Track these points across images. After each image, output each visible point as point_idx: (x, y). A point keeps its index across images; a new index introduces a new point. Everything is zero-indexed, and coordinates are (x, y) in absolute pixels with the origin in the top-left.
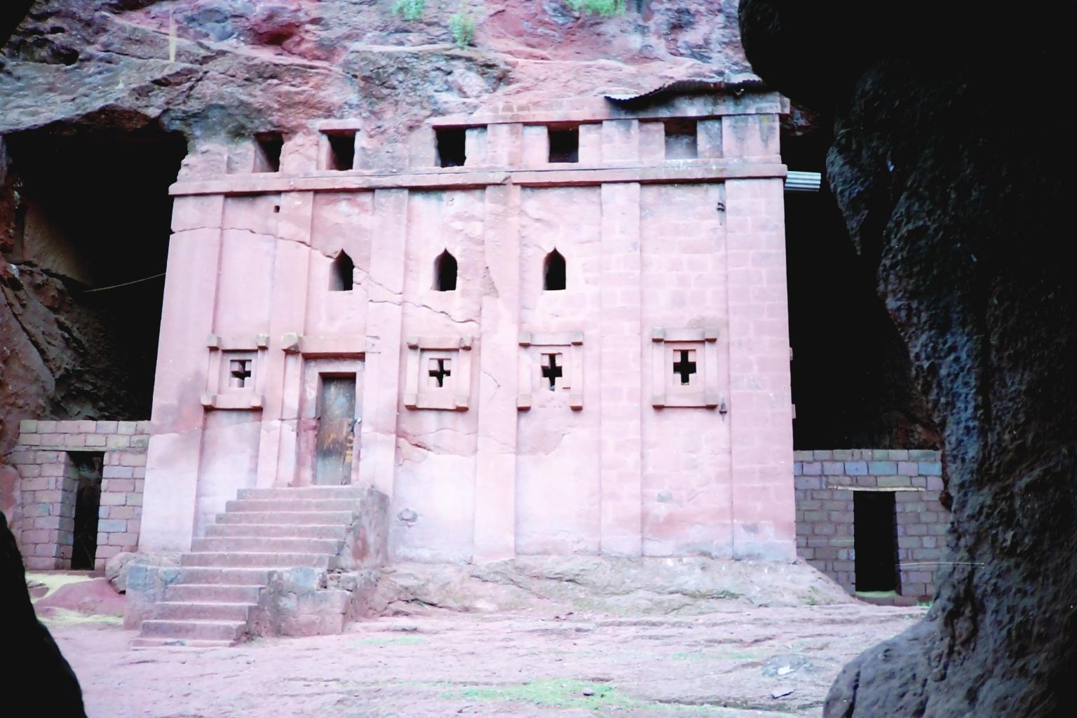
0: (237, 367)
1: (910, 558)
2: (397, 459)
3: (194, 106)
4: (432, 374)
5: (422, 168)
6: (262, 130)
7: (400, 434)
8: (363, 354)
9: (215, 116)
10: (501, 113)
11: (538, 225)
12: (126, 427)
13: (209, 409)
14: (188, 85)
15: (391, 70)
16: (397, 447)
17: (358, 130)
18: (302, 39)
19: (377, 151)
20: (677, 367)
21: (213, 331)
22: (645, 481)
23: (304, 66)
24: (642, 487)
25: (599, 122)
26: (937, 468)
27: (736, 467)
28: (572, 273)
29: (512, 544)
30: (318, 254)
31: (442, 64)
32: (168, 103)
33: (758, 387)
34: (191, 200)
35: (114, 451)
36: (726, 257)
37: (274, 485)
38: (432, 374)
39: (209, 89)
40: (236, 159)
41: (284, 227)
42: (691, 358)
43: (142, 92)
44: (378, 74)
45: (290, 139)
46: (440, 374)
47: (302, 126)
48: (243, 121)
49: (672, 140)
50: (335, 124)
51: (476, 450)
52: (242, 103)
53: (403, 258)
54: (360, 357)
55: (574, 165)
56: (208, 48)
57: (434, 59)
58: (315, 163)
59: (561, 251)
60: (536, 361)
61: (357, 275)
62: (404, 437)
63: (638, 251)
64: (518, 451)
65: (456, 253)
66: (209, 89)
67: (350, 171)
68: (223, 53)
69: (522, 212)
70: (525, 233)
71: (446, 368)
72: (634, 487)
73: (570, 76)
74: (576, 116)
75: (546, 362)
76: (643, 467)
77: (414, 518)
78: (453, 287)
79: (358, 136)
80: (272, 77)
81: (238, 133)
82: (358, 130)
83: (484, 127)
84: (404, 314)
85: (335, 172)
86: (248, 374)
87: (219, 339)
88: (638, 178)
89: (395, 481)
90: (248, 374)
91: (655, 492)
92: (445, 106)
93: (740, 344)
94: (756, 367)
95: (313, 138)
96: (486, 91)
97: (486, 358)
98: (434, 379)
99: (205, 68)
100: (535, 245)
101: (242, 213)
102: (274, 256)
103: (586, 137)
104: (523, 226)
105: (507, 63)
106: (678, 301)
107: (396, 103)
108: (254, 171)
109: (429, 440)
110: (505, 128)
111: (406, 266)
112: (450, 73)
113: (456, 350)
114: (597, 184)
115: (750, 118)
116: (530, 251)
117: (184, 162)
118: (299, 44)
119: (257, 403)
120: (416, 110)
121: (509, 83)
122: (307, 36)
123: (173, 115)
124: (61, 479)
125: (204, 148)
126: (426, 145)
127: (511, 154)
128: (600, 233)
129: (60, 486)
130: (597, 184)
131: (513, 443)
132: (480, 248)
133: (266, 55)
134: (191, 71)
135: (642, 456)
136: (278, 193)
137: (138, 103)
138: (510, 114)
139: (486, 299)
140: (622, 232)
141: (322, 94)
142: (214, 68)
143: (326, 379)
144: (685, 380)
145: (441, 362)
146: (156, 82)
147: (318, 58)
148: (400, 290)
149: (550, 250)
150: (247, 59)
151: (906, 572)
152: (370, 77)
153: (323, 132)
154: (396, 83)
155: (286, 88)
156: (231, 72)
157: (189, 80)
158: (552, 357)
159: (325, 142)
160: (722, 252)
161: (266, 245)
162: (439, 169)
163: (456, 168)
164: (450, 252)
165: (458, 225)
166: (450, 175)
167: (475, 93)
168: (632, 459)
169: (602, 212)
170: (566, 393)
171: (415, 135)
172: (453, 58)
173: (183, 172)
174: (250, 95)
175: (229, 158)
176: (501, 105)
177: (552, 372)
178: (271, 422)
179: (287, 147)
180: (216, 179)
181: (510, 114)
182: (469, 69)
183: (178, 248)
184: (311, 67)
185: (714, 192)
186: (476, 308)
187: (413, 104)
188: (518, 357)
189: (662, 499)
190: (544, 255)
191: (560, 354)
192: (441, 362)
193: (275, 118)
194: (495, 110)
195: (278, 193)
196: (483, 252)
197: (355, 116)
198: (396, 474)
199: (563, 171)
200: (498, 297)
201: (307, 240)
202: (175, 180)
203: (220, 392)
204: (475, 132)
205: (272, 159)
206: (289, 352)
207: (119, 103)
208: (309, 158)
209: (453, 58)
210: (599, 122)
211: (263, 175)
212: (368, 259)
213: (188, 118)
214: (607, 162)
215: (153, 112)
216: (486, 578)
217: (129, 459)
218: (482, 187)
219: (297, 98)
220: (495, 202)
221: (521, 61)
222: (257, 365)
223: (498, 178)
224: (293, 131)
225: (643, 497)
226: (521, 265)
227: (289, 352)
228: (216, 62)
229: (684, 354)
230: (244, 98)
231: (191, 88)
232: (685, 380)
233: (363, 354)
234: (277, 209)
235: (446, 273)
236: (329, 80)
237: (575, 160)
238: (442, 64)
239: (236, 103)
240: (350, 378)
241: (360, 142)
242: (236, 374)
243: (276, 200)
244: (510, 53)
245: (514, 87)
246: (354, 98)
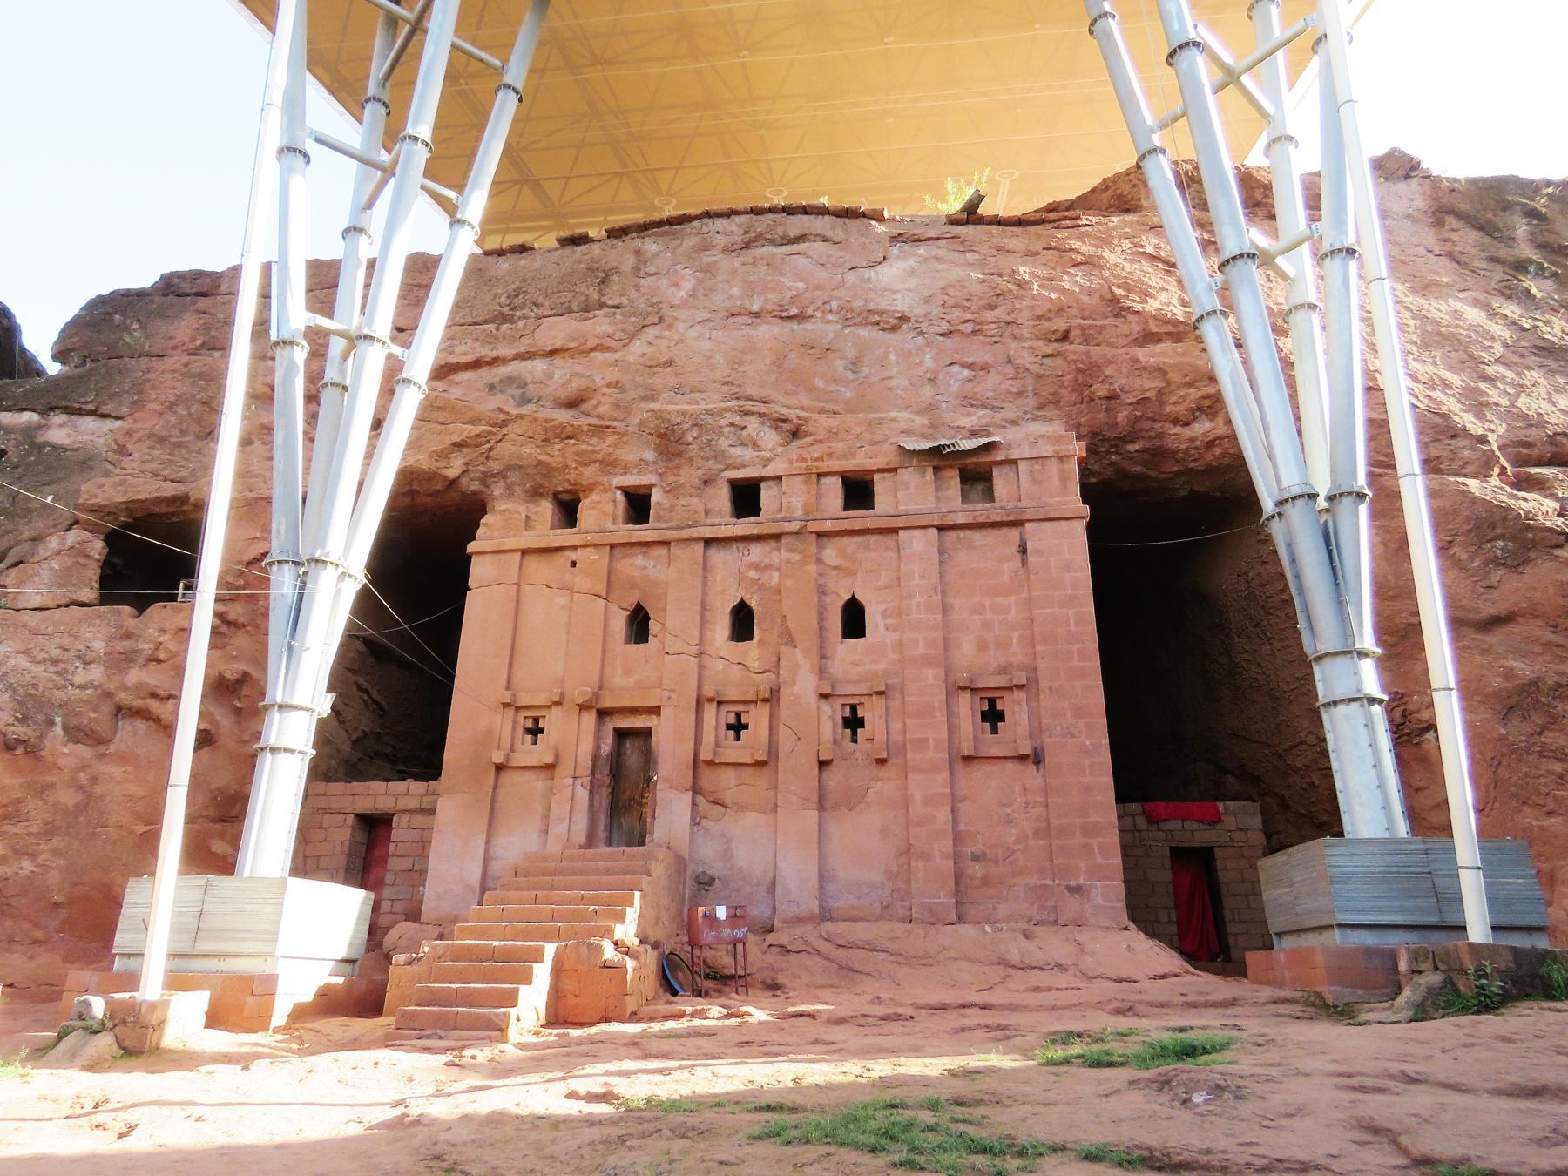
0: (530, 724)
1: (1237, 918)
2: (693, 818)
3: (494, 466)
4: (729, 727)
5: (717, 520)
6: (561, 489)
7: (696, 790)
8: (659, 707)
9: (513, 477)
10: (795, 465)
11: (835, 572)
12: (417, 787)
13: (499, 768)
14: (488, 446)
15: (685, 427)
16: (694, 804)
17: (654, 485)
18: (599, 403)
19: (672, 508)
20: (985, 716)
21: (508, 688)
22: (958, 838)
23: (601, 426)
24: (954, 845)
25: (893, 470)
26: (1256, 822)
27: (1054, 822)
28: (872, 619)
29: (817, 910)
30: (614, 607)
31: (737, 419)
32: (467, 464)
33: (1073, 736)
34: (489, 558)
35: (404, 811)
36: (1030, 600)
37: (565, 848)
38: (729, 727)
39: (506, 450)
40: (533, 516)
41: (581, 581)
42: (999, 707)
43: (442, 455)
44: (673, 430)
45: (587, 497)
46: (738, 727)
47: (600, 484)
48: (539, 479)
49: (967, 487)
50: (631, 480)
51: (776, 807)
52: (540, 463)
53: (698, 608)
54: (655, 711)
55: (871, 512)
56: (508, 414)
57: (727, 415)
58: (611, 519)
59: (859, 597)
60: (836, 711)
61: (654, 626)
62: (701, 794)
63: (939, 597)
64: (821, 807)
65: (753, 604)
66: (506, 450)
67: (646, 525)
68: (522, 417)
69: (819, 561)
70: (822, 581)
71: (743, 721)
72: (947, 845)
73: (863, 429)
74: (870, 464)
75: (848, 713)
76: (955, 821)
77: (713, 879)
78: (750, 638)
79: (654, 491)
80: (569, 437)
81: (535, 494)
82: (654, 485)
83: (779, 478)
84: (701, 667)
85: (631, 526)
86: (542, 731)
87: (514, 696)
88: (936, 523)
89: (691, 841)
90: (542, 731)
91: (968, 851)
92: (739, 460)
93: (1050, 689)
94: (1069, 714)
95: (609, 494)
96: (781, 445)
97: (785, 711)
98: (731, 733)
99: (504, 430)
100: (833, 593)
101: (539, 569)
102: (571, 610)
103: (881, 486)
104: (821, 575)
105: (799, 418)
106: (982, 646)
107: (691, 459)
108: (552, 527)
109: (728, 797)
110: (799, 479)
111: (702, 616)
112: (743, 428)
113: (755, 702)
114: (894, 531)
115: (1048, 462)
116: (828, 599)
117: (482, 521)
118: (596, 407)
119: (549, 760)
120: (710, 463)
121: (805, 436)
122: (603, 400)
123: (472, 475)
124: (347, 844)
125: (504, 507)
127: (806, 505)
128: (899, 579)
129: (346, 849)
130: (894, 531)
131: (815, 797)
132: (778, 597)
133: (563, 416)
134: (490, 433)
135: (953, 811)
136: (575, 548)
137: (438, 464)
138: (804, 465)
139: (783, 649)
140: (922, 577)
141: (618, 452)
142: (515, 430)
143: (621, 734)
144: (995, 730)
145: (738, 716)
146: (455, 444)
147: (615, 420)
148: (697, 641)
149: (848, 597)
150: (547, 421)
151: (1235, 935)
152: (665, 434)
153: (621, 488)
154: (690, 439)
155: (583, 447)
156: (529, 434)
157: (488, 442)
158: (854, 708)
159: (619, 496)
160: (1025, 595)
161: (562, 600)
162: (734, 520)
163: (752, 519)
164: (747, 601)
165: (753, 574)
166: (746, 526)
167: (770, 446)
168: (943, 815)
169: (900, 558)
170: (869, 745)
171: (709, 490)
172: (747, 413)
173: (481, 531)
174: (548, 454)
175: (527, 517)
176: (794, 457)
177: (854, 722)
178: (564, 778)
179: (584, 504)
180: (514, 536)
181: (804, 465)
182: (763, 423)
183: (475, 605)
184: (607, 427)
185: (1014, 534)
186: (774, 659)
187: (707, 459)
188: (818, 708)
189: (976, 858)
190: (842, 603)
191: (861, 704)
192: (738, 716)
193: (572, 477)
194: (791, 462)
195: (575, 548)
196: (780, 601)
197: (651, 472)
198: (692, 833)
199: (858, 519)
200: (795, 647)
201: (604, 594)
202: (473, 539)
203: (512, 750)
204: (771, 483)
206: (583, 707)
207: (418, 464)
208: (606, 514)
209: (747, 413)
210: (893, 470)
211: (559, 531)
212: (664, 610)
213: (486, 478)
214: (902, 508)
215: (452, 473)
216: (789, 948)
217: (418, 820)
218: (777, 537)
219: (594, 457)
220: (789, 550)
221: (815, 416)
222: (553, 722)
223: (794, 526)
224: (590, 489)
225: (957, 857)
226: (820, 614)
227: (583, 707)
228: (516, 425)
229: (992, 702)
230: (541, 457)
231: (490, 450)
232: (995, 730)
233: (659, 707)
234: (574, 564)
235: (743, 622)
236: (625, 439)
237: (871, 507)
238: (737, 419)
239: (534, 463)
240: (646, 733)
241: (656, 496)
242: (529, 731)
243: (573, 555)
244: (802, 408)
245: (808, 440)
246: (650, 455)
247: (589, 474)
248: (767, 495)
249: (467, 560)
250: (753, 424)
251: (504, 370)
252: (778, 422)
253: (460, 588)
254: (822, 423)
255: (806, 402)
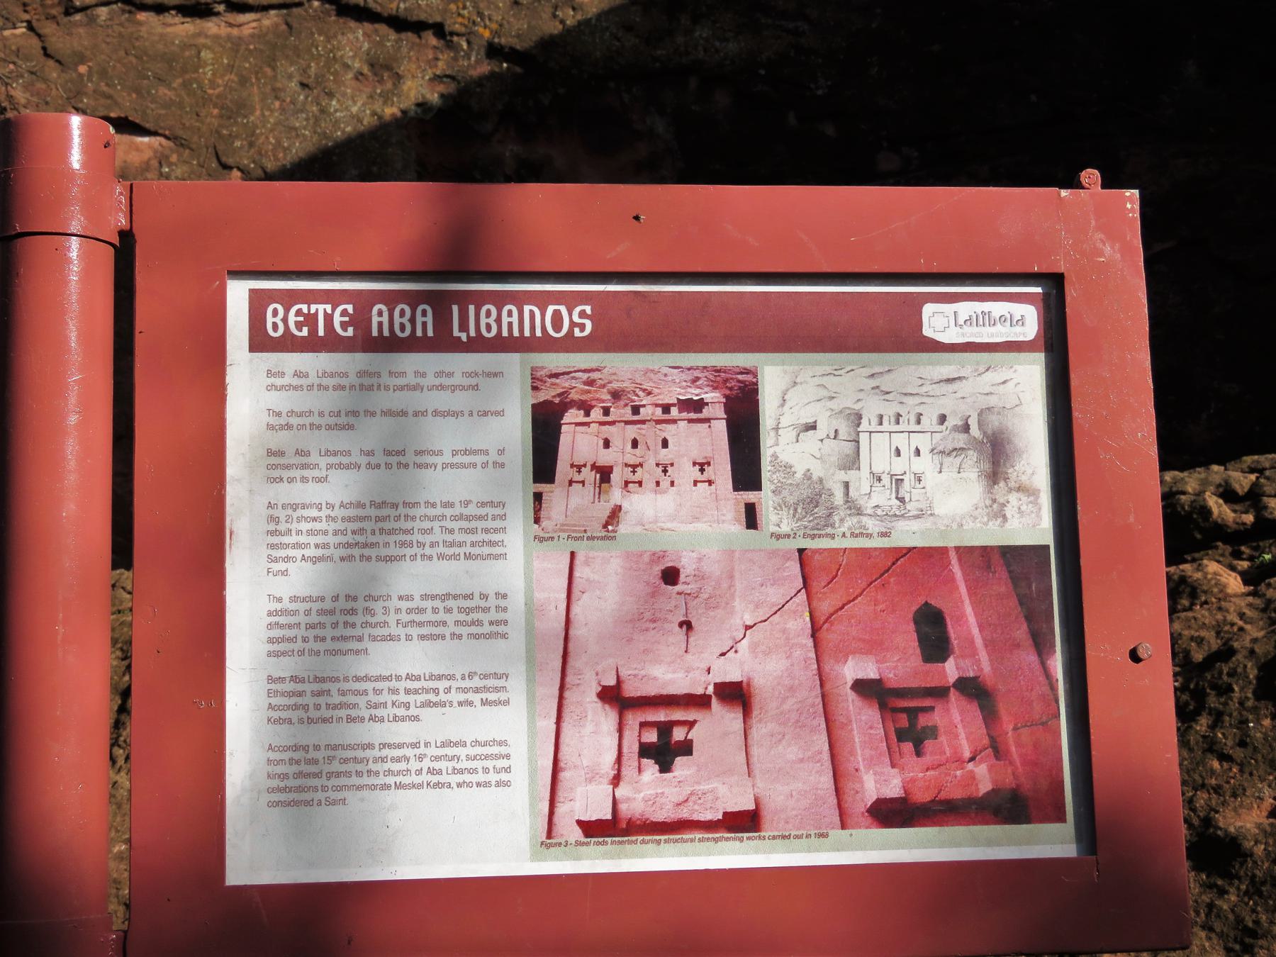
43: (554, 397)
81: (579, 409)
109: (631, 490)
126: (629, 410)
144: (702, 474)
205: (587, 414)
232: (702, 474)
235: (635, 444)
247: (594, 403)
248: (642, 410)
249: (560, 425)
250: (637, 390)
251: (572, 375)
252: (644, 390)
253: (560, 433)
254: (656, 391)
255: (653, 385)
